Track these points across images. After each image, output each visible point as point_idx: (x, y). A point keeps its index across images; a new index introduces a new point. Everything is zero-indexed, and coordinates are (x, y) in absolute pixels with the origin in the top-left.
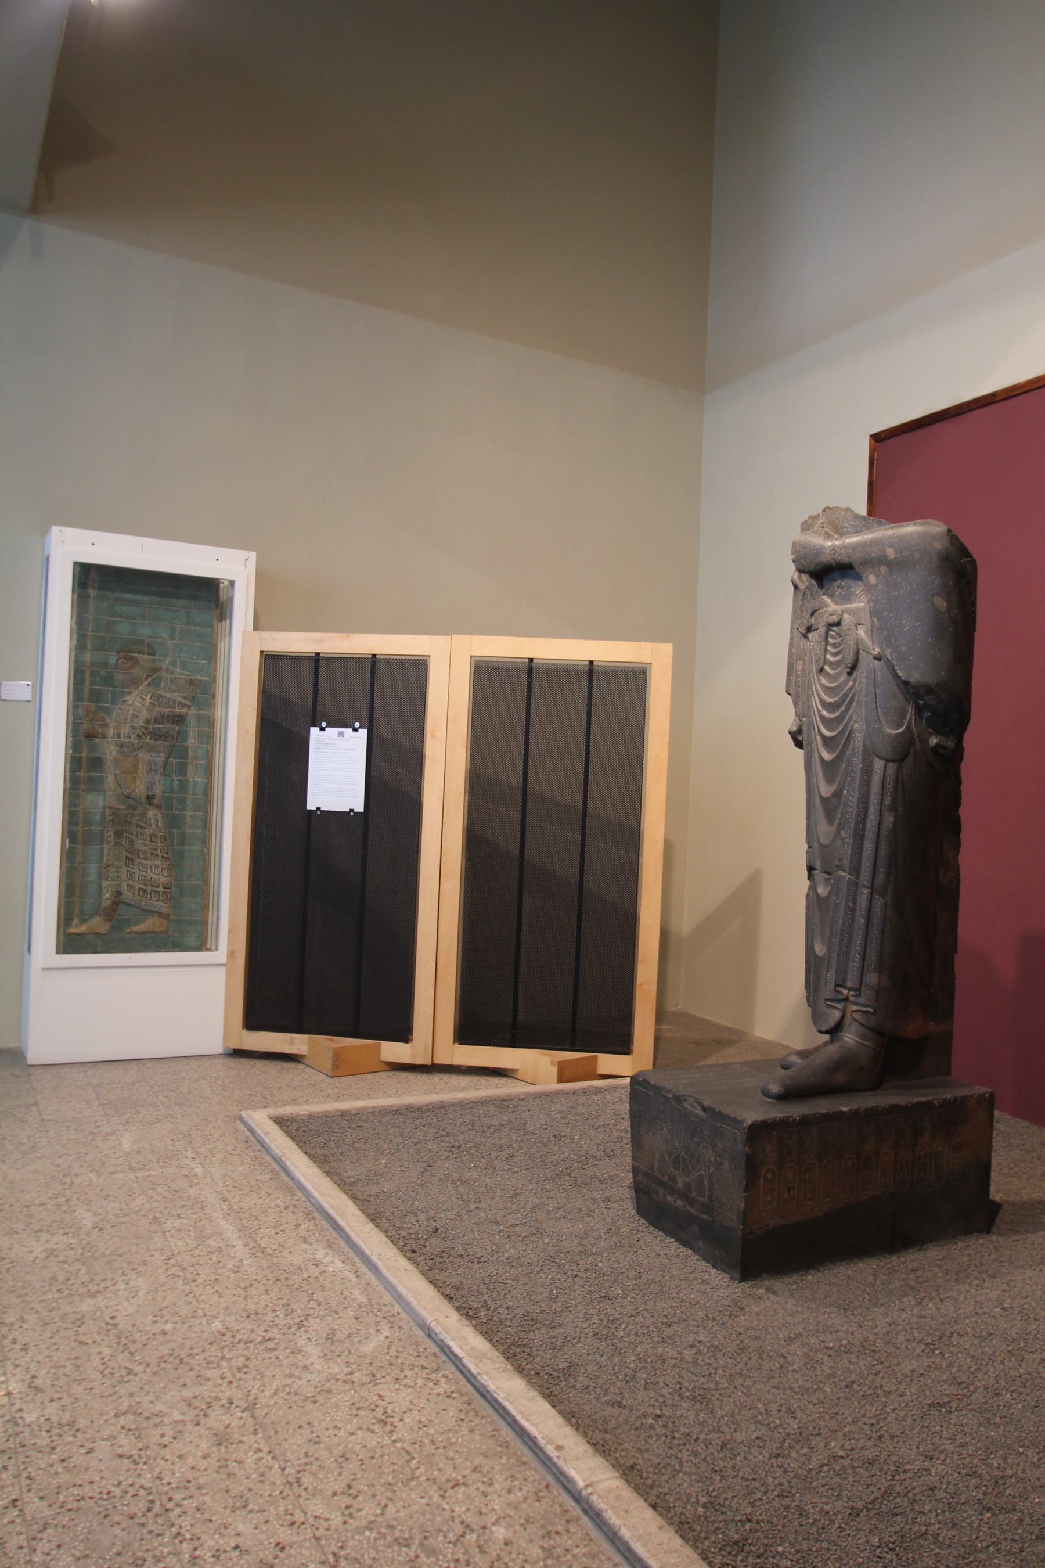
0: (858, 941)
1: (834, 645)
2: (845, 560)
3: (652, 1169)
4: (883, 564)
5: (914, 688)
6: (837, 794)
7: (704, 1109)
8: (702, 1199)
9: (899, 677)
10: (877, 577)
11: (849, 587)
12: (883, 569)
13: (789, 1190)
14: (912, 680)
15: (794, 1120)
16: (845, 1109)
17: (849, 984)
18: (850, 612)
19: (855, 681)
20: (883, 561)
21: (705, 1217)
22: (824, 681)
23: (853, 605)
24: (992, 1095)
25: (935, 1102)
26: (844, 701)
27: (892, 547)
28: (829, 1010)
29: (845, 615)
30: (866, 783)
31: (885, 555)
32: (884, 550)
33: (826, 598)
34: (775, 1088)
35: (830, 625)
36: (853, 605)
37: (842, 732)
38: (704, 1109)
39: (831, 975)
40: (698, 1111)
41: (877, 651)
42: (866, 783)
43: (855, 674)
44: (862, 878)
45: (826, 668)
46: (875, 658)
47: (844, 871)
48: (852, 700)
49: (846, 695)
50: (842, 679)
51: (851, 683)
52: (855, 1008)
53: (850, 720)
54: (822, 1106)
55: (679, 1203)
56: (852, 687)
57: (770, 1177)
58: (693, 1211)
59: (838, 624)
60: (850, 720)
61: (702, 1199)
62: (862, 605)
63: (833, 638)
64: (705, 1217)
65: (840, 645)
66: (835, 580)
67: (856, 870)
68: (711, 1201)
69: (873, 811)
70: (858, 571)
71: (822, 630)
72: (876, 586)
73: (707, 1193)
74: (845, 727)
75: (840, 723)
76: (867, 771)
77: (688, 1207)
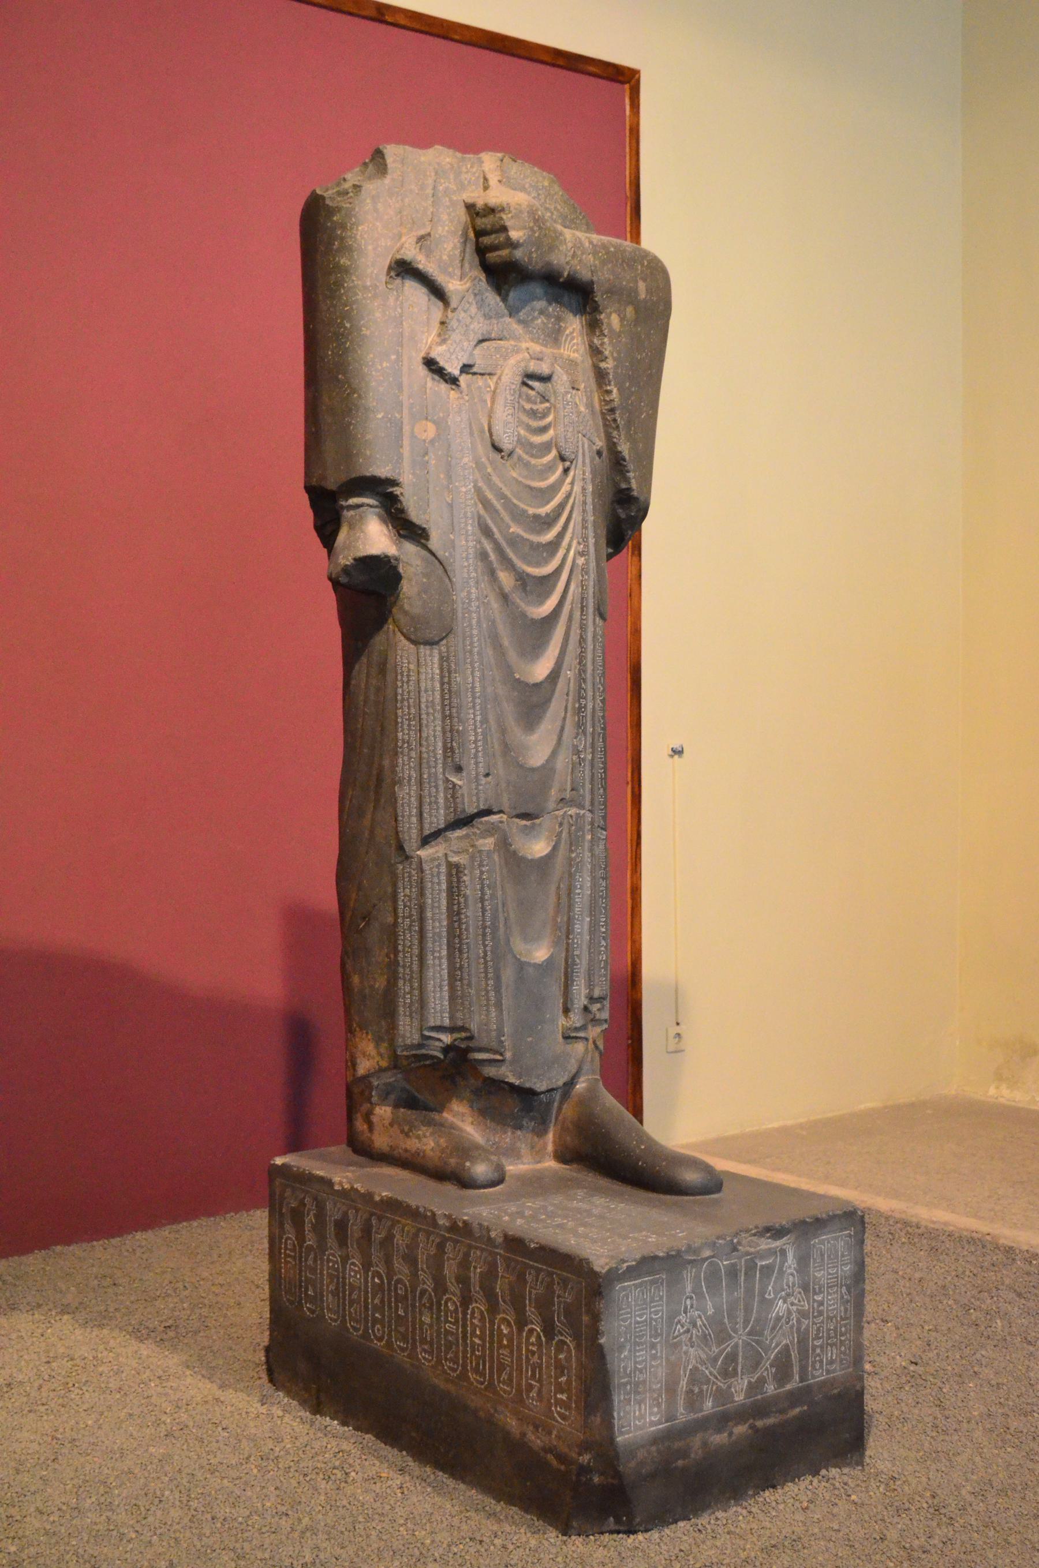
4: (631, 303)
9: (629, 489)
10: (622, 320)
11: (559, 319)
12: (630, 311)
19: (572, 483)
21: (797, 1410)
26: (559, 515)
27: (645, 280)
28: (569, 1047)
32: (637, 282)
37: (558, 571)
43: (571, 473)
45: (519, 451)
47: (581, 806)
49: (561, 506)
50: (553, 479)
56: (568, 496)
58: (770, 1421)
59: (545, 379)
62: (574, 356)
63: (529, 400)
64: (797, 1410)
77: (759, 1424)
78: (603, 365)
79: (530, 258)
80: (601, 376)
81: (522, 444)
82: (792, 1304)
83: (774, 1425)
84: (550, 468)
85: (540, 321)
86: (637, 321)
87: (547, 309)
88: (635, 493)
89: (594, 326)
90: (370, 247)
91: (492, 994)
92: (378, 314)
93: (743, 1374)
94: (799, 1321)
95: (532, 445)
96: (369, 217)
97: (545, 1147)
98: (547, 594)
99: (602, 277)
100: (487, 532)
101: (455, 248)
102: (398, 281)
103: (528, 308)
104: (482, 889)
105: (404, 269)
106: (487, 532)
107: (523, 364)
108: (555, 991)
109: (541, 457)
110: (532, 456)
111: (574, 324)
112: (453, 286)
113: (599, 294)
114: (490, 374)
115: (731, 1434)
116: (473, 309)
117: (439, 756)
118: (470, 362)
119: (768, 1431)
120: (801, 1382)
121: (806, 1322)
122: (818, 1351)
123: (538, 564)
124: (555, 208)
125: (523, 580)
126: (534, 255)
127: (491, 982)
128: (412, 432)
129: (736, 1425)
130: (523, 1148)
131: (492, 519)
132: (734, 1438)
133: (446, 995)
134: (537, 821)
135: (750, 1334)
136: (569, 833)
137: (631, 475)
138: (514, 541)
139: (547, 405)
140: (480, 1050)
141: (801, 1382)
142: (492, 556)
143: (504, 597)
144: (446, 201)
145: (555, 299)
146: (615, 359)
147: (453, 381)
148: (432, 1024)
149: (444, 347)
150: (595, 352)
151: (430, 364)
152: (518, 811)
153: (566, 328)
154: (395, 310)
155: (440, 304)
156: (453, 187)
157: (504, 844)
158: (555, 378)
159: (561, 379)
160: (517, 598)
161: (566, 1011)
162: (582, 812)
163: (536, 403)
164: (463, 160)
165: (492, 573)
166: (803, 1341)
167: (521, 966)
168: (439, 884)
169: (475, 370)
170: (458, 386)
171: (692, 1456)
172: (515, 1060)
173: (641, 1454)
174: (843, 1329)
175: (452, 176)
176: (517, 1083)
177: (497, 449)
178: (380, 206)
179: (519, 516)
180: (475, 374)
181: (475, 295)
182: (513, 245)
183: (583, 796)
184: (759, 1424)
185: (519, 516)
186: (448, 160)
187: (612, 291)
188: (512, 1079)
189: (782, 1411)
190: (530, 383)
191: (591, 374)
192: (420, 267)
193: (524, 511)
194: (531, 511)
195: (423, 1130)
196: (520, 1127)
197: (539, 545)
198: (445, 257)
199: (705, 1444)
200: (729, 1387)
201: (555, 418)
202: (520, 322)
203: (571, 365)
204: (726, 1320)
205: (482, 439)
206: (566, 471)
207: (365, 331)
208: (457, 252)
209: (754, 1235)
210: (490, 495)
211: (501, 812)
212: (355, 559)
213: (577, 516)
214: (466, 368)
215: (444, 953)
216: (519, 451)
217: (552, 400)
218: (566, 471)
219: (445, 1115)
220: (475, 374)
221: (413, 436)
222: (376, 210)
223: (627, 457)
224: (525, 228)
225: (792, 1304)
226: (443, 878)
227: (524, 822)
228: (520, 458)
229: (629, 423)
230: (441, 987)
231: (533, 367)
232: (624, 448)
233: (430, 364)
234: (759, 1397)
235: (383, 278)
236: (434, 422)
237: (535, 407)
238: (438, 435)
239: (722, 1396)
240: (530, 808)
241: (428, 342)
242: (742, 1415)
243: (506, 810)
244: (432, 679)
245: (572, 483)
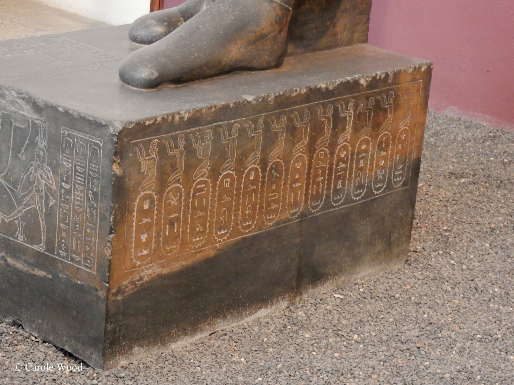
7: (37, 108)
8: (35, 247)
13: (172, 225)
15: (181, 118)
16: (250, 98)
21: (41, 273)
24: (429, 70)
25: (362, 82)
34: (145, 73)
38: (37, 108)
40: (27, 112)
54: (249, 91)
57: (146, 207)
58: (19, 266)
61: (35, 247)
64: (41, 273)
68: (50, 248)
73: (43, 238)
77: (10, 260)
83: (22, 271)
119: (16, 271)
120: (46, 251)
121: (54, 201)
122: (64, 234)
141: (46, 251)
166: (50, 214)
174: (88, 231)
184: (10, 260)
209: (24, 99)
234: (11, 239)
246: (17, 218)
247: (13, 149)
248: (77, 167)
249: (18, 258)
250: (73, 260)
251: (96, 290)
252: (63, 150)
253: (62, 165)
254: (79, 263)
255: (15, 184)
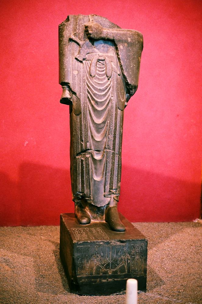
0: (116, 173)
1: (100, 68)
2: (112, 38)
3: (91, 274)
4: (126, 43)
5: (132, 86)
6: (104, 122)
8: (124, 274)
9: (128, 82)
10: (123, 47)
12: (126, 44)
14: (132, 84)
17: (114, 188)
18: (108, 57)
19: (111, 82)
20: (126, 41)
22: (95, 81)
23: (109, 54)
26: (107, 89)
27: (130, 38)
28: (106, 198)
29: (106, 57)
30: (116, 118)
31: (127, 40)
32: (127, 38)
33: (95, 49)
35: (99, 60)
36: (109, 54)
37: (106, 100)
39: (108, 187)
40: (119, 243)
41: (119, 73)
42: (116, 118)
43: (110, 79)
44: (116, 151)
45: (96, 76)
46: (118, 75)
48: (110, 88)
49: (107, 87)
51: (109, 83)
52: (115, 196)
53: (109, 96)
55: (110, 280)
56: (110, 84)
59: (104, 60)
60: (109, 96)
62: (112, 55)
63: (99, 65)
65: (103, 68)
66: (101, 44)
67: (114, 149)
69: (118, 128)
70: (116, 43)
71: (94, 61)
72: (123, 50)
74: (107, 98)
75: (105, 97)
76: (116, 114)
77: (116, 279)
78: (119, 57)
79: (95, 37)
80: (119, 59)
81: (97, 74)
82: (125, 257)
83: (120, 280)
84: (104, 79)
85: (102, 48)
86: (128, 47)
87: (104, 46)
88: (130, 83)
89: (117, 49)
90: (65, 36)
91: (88, 186)
92: (66, 50)
93: (111, 269)
94: (127, 261)
95: (100, 74)
96: (65, 30)
97: (103, 217)
98: (104, 105)
99: (116, 38)
100: (89, 92)
101: (82, 35)
102: (70, 42)
103: (99, 46)
104: (87, 165)
105: (71, 40)
106: (89, 92)
107: (97, 58)
108: (102, 187)
109: (102, 77)
110: (100, 76)
111: (112, 49)
112: (81, 43)
113: (116, 42)
114: (90, 60)
115: (108, 280)
116: (86, 47)
117: (79, 138)
118: (86, 58)
123: (101, 99)
124: (107, 24)
125: (97, 102)
126: (96, 36)
127: (88, 184)
128: (73, 72)
129: (109, 279)
130: (99, 218)
131: (90, 90)
132: (108, 281)
133: (81, 185)
134: (100, 152)
135: (113, 261)
136: (107, 155)
137: (128, 79)
138: (95, 94)
139: (104, 66)
140: (87, 197)
142: (90, 98)
143: (92, 106)
144: (81, 25)
145: (105, 43)
146: (121, 55)
147: (81, 62)
148: (78, 191)
149: (79, 55)
150: (118, 54)
151: (76, 59)
152: (96, 150)
153: (110, 49)
154: (70, 48)
155: (79, 46)
156: (82, 22)
157: (92, 156)
158: (105, 60)
159: (107, 60)
160: (96, 106)
161: (105, 191)
162: (110, 151)
163: (101, 65)
164: (85, 17)
165: (90, 101)
166: (128, 264)
167: (95, 181)
168: (79, 164)
169: (86, 59)
170: (83, 63)
171: (97, 283)
172: (93, 200)
173: (83, 280)
175: (82, 20)
176: (94, 204)
177: (91, 76)
178: (68, 28)
179: (96, 89)
180: (87, 60)
181: (86, 44)
182: (90, 34)
183: (111, 147)
184: (116, 279)
185: (96, 89)
186: (82, 17)
187: (120, 41)
188: (93, 204)
189: (122, 278)
190: (99, 61)
191: (117, 58)
192: (74, 39)
193: (97, 88)
194: (99, 88)
195: (80, 212)
196: (98, 214)
197: (101, 95)
198: (80, 37)
199: (100, 281)
200: (108, 271)
201: (106, 69)
202: (97, 49)
203: (111, 57)
204: (107, 257)
205: (88, 74)
206: (109, 79)
207: (64, 53)
208: (83, 36)
210: (89, 85)
211: (91, 150)
212: (62, 98)
213: (111, 88)
214: (84, 59)
215: (80, 177)
216: (96, 76)
217: (105, 65)
218: (109, 79)
219: (85, 209)
220: (87, 60)
221: (73, 74)
222: (67, 28)
223: (126, 76)
224: (92, 30)
225: (125, 257)
226: (80, 162)
227: (98, 152)
228: (97, 77)
229: (126, 69)
230: (80, 184)
231: (100, 58)
232: (125, 74)
233: (76, 59)
235: (68, 42)
236: (77, 70)
237: (101, 66)
238: (78, 73)
239: (106, 273)
240: (98, 149)
241: (76, 55)
242: (110, 277)
243: (93, 149)
244: (78, 122)
245: (111, 82)
246: (118, 269)
247: (116, 253)
248: (137, 251)
249: (118, 278)
250: (136, 272)
251: (144, 276)
252: (132, 249)
253: (132, 252)
254: (138, 272)
255: (117, 261)
